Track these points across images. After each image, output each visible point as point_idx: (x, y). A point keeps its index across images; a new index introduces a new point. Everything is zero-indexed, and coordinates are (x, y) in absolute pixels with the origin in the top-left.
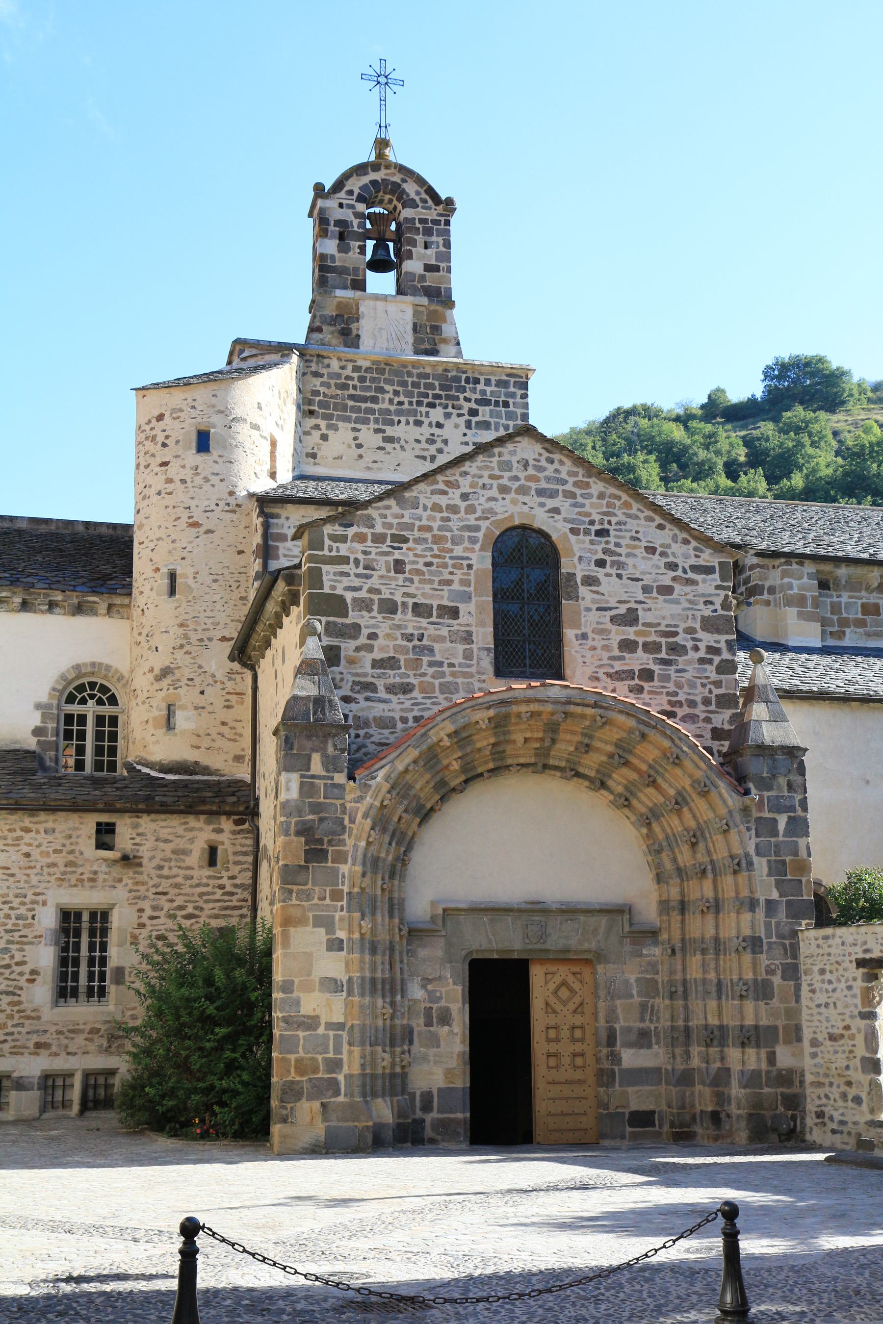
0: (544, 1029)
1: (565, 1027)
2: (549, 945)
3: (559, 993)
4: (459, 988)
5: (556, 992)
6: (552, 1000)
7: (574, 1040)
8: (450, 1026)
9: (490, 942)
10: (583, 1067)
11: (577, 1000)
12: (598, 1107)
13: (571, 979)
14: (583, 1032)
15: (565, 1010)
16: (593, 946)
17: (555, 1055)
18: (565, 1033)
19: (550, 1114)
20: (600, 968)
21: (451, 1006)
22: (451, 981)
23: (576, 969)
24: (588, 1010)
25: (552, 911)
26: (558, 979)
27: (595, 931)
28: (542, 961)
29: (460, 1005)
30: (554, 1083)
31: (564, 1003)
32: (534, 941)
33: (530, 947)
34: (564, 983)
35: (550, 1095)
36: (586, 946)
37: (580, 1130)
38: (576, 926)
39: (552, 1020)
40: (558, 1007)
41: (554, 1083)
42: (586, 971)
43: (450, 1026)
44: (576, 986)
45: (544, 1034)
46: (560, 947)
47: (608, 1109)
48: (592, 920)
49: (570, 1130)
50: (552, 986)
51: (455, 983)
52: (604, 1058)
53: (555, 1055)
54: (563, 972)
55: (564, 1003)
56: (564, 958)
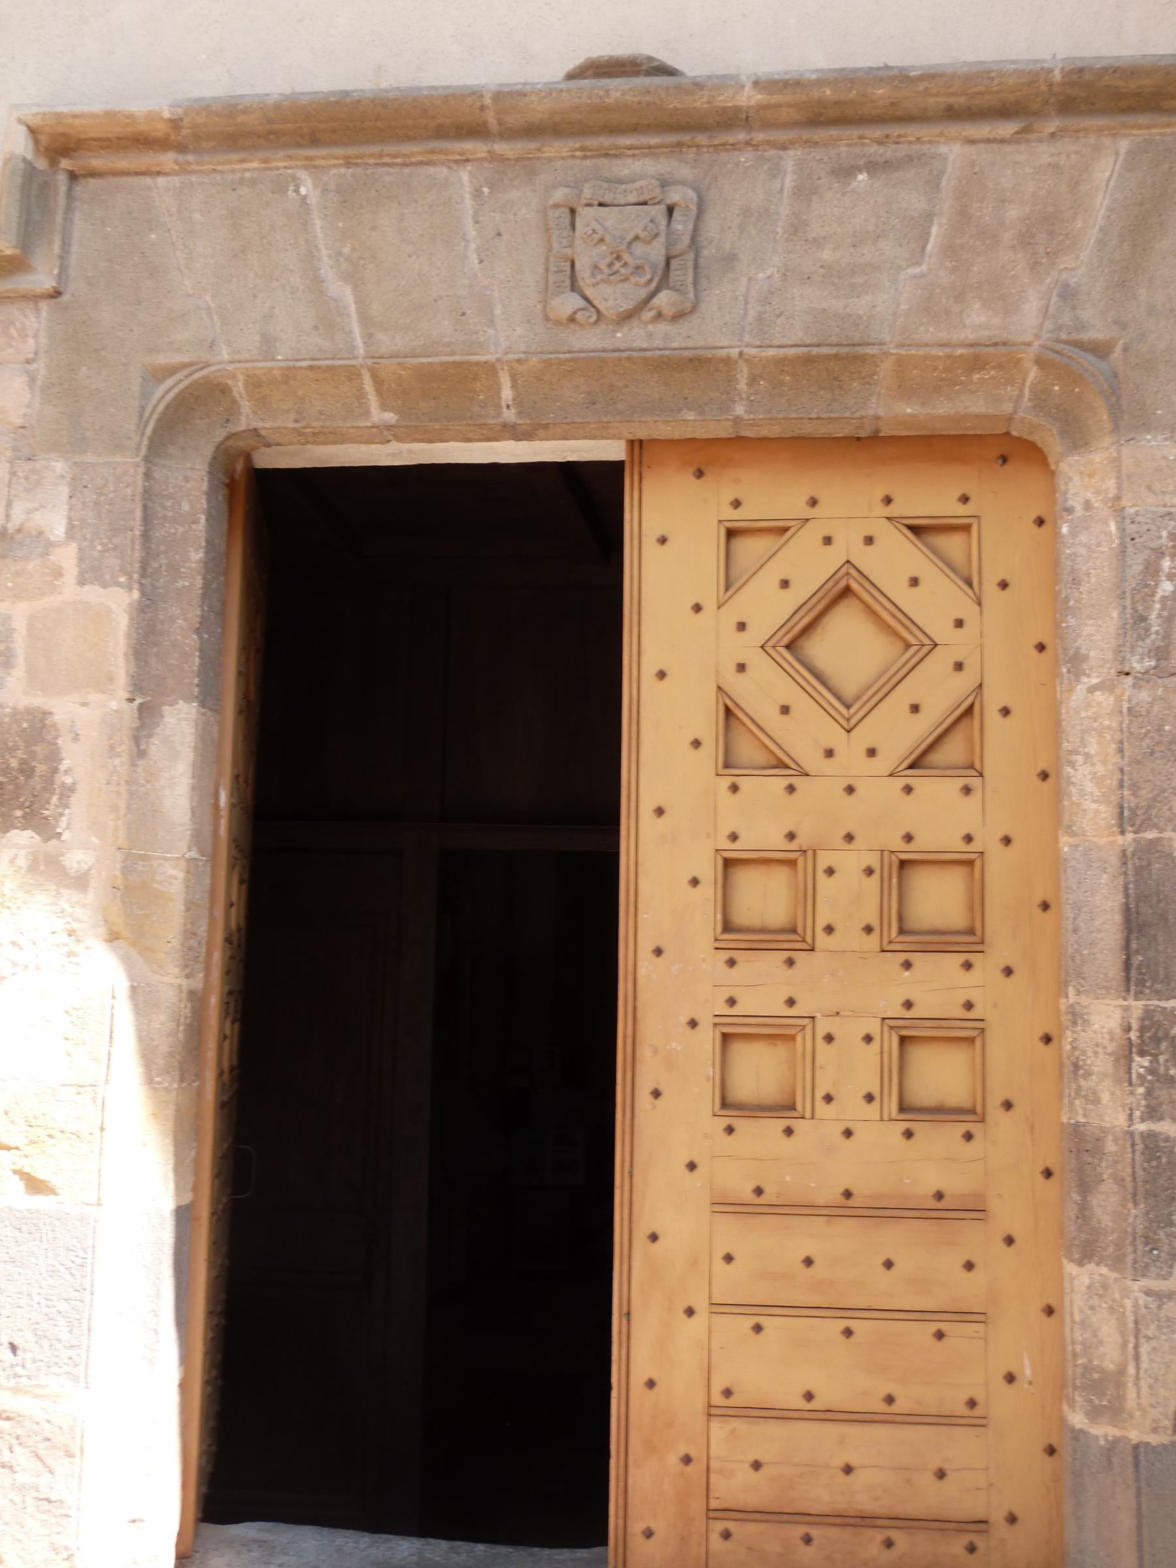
0: (708, 871)
1: (850, 862)
2: (724, 322)
3: (819, 648)
4: (118, 603)
5: (794, 641)
6: (765, 689)
7: (908, 939)
8: (46, 829)
9: (328, 319)
10: (967, 1115)
11: (937, 690)
12: (1061, 1387)
13: (893, 562)
14: (977, 901)
15: (851, 749)
16: (1029, 319)
17: (777, 1034)
18: (848, 895)
19: (726, 1406)
20: (1086, 480)
21: (64, 710)
22: (67, 557)
23: (932, 496)
24: (1001, 742)
25: (731, 119)
26: (808, 566)
27: (1046, 232)
28: (704, 456)
29: (116, 702)
30: (757, 1205)
31: (850, 709)
32: (613, 297)
33: (590, 340)
34: (840, 593)
35: (728, 1282)
36: (977, 322)
37: (939, 1524)
38: (913, 201)
39: (761, 815)
40: (807, 731)
41: (757, 1205)
42: (999, 510)
43: (46, 829)
44: (934, 603)
45: (708, 891)
46: (792, 333)
47: (1115, 1411)
48: (1021, 169)
49: (863, 1521)
50: (768, 607)
51: (90, 574)
52: (1101, 1064)
53: (777, 1034)
54: (848, 521)
55: (850, 709)
56: (834, 422)
